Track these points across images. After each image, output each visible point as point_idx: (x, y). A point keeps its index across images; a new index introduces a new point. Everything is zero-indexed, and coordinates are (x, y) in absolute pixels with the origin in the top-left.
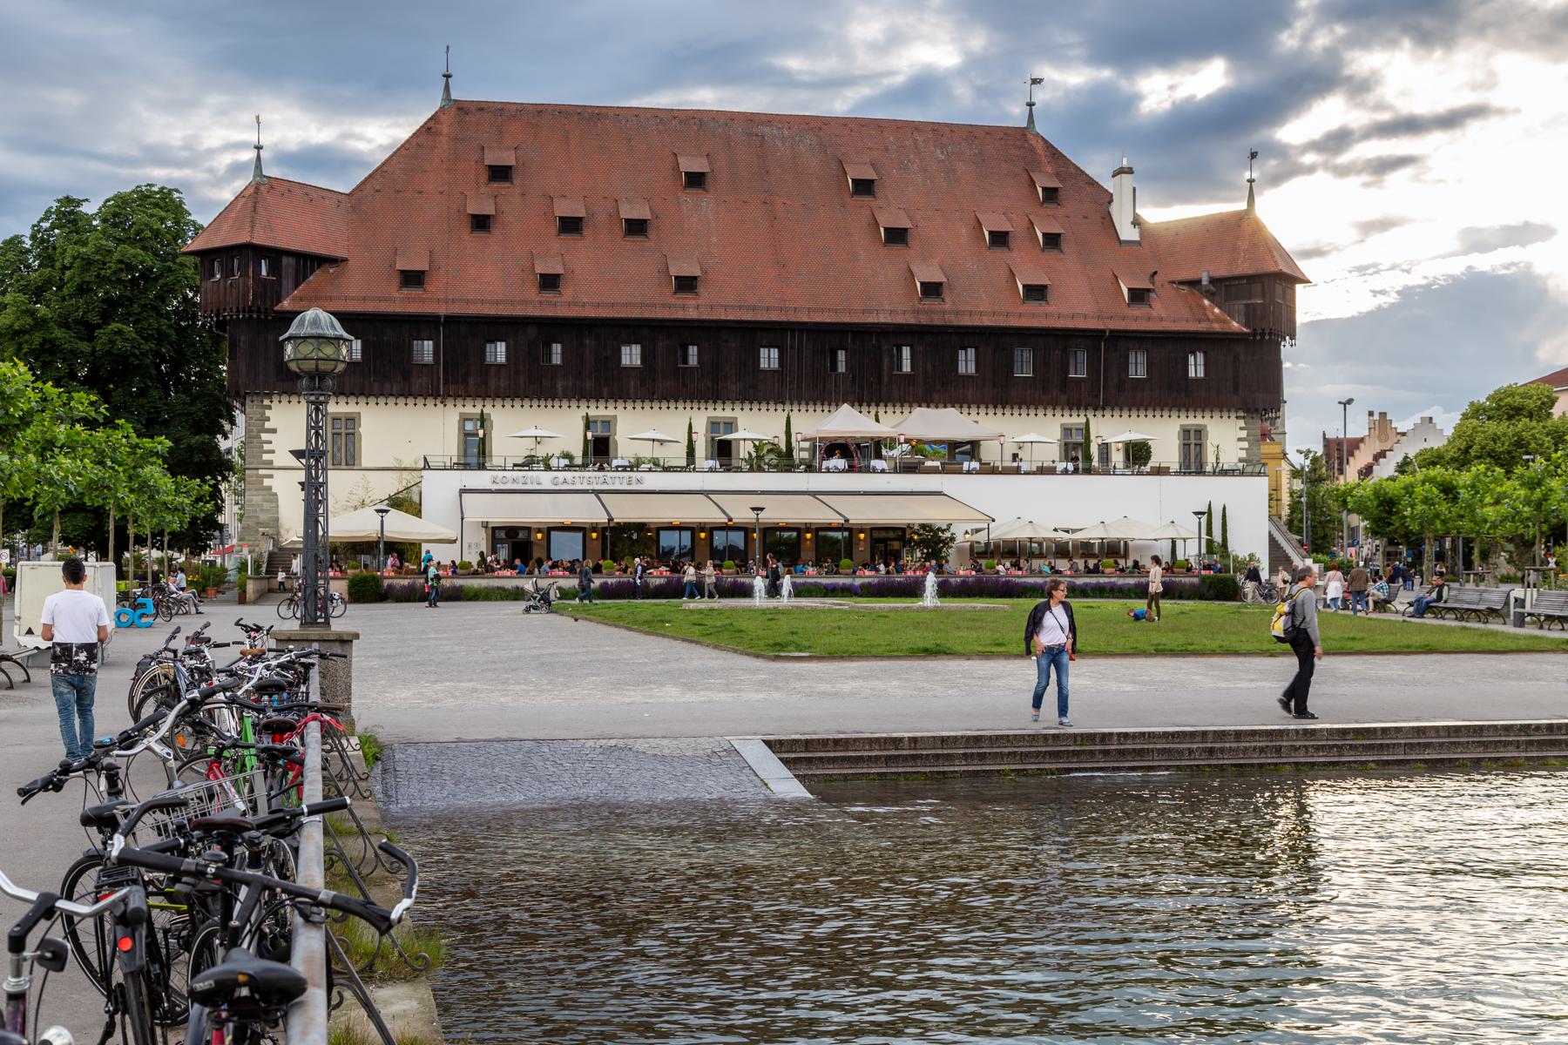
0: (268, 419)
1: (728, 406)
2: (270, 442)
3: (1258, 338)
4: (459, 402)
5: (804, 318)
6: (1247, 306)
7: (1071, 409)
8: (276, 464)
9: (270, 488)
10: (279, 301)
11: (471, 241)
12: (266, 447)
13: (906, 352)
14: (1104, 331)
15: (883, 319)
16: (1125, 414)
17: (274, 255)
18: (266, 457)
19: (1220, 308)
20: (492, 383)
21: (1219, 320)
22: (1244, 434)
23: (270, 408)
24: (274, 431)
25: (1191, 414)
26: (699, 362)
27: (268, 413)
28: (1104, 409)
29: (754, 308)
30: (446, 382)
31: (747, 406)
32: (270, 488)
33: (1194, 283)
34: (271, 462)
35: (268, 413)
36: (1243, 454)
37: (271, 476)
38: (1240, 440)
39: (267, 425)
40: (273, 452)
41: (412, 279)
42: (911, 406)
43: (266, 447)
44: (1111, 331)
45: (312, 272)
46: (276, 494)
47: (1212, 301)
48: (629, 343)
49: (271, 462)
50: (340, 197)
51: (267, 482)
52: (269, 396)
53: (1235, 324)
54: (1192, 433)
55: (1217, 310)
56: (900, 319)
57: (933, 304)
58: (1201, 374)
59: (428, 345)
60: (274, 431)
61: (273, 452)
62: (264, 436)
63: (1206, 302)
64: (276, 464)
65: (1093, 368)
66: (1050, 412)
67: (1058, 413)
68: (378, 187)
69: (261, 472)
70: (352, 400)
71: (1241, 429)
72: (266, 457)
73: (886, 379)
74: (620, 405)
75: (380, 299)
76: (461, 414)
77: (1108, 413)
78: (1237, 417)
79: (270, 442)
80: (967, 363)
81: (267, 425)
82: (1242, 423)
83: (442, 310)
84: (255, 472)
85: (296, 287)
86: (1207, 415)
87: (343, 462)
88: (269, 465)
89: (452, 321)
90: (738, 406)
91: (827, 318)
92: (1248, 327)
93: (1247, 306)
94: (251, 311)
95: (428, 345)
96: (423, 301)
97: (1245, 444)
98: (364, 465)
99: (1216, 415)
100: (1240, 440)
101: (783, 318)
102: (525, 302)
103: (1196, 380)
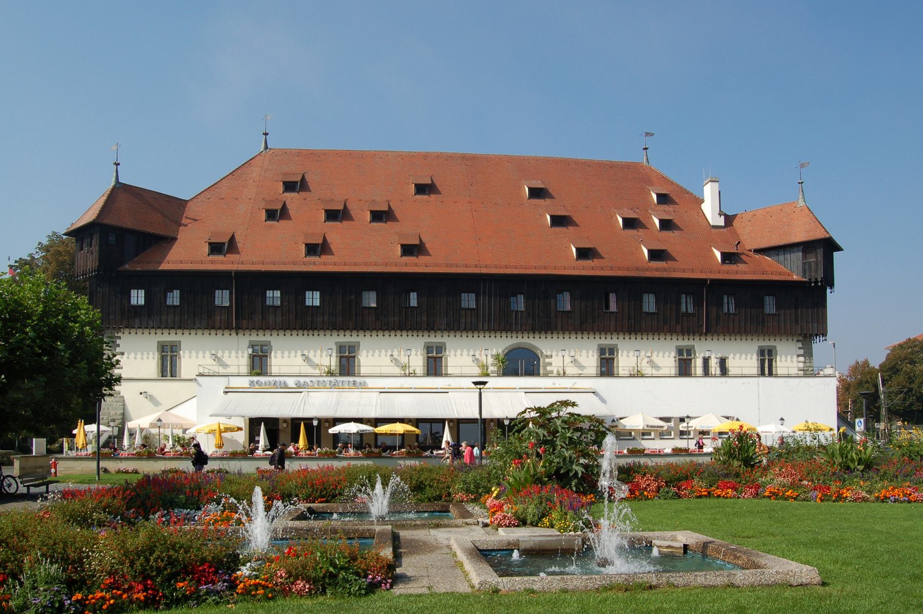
0: (119, 346)
1: (439, 334)
4: (247, 333)
14: (706, 280)
16: (721, 338)
20: (271, 319)
22: (801, 352)
23: (120, 338)
25: (766, 339)
26: (418, 304)
27: (118, 342)
28: (706, 334)
31: (452, 334)
35: (118, 342)
36: (801, 365)
44: (712, 280)
54: (766, 352)
66: (669, 338)
67: (674, 338)
71: (800, 348)
76: (250, 341)
77: (709, 338)
78: (798, 341)
81: (118, 350)
85: (136, 255)
86: (778, 338)
87: (169, 374)
90: (446, 334)
92: (805, 278)
97: (802, 359)
98: (183, 377)
99: (784, 340)
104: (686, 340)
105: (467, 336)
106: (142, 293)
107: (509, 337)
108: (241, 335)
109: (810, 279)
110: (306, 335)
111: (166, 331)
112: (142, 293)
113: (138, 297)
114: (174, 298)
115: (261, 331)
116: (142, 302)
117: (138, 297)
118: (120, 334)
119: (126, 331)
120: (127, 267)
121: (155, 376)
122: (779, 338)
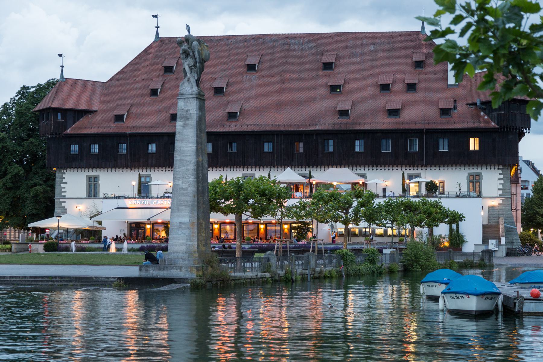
0: (64, 178)
2: (64, 188)
3: (502, 130)
5: (282, 129)
6: (498, 115)
7: (410, 167)
8: (67, 197)
9: (64, 207)
10: (66, 130)
11: (149, 100)
12: (63, 190)
13: (331, 142)
14: (423, 130)
15: (318, 128)
17: (64, 111)
18: (63, 194)
19: (488, 116)
21: (486, 122)
22: (501, 176)
23: (65, 173)
24: (66, 183)
27: (64, 176)
29: (260, 125)
30: (131, 161)
32: (64, 207)
33: (475, 104)
34: (65, 196)
35: (64, 176)
37: (65, 202)
38: (499, 179)
39: (64, 181)
40: (65, 192)
41: (119, 118)
42: (285, 167)
43: (63, 190)
44: (427, 130)
45: (81, 117)
46: (66, 209)
47: (485, 112)
48: (268, 142)
49: (65, 196)
50: (101, 84)
51: (63, 204)
52: (64, 169)
53: (493, 124)
55: (486, 117)
56: (325, 128)
57: (345, 120)
58: (477, 148)
59: (125, 146)
60: (66, 183)
61: (65, 192)
62: (63, 185)
63: (482, 113)
64: (67, 197)
65: (420, 147)
68: (118, 79)
69: (61, 200)
70: (94, 170)
71: (500, 174)
72: (63, 194)
73: (320, 156)
74: (152, 170)
75: (105, 128)
77: (429, 169)
78: (498, 169)
79: (64, 188)
80: (358, 146)
81: (64, 181)
82: (500, 171)
83: (128, 131)
84: (59, 200)
87: (93, 195)
88: (64, 197)
89: (132, 135)
91: (292, 129)
93: (498, 115)
94: (52, 134)
95: (125, 146)
96: (122, 127)
97: (502, 182)
100: (499, 179)
101: (272, 129)
102: (222, 125)
103: (474, 151)
104: (415, 170)
105: (381, 170)
106: (77, 146)
107: (232, 170)
108: (133, 171)
109: (501, 126)
110: (170, 171)
111: (90, 170)
112: (77, 146)
113: (75, 149)
114: (95, 149)
115: (87, 168)
116: (77, 152)
117: (75, 149)
118: (65, 171)
119: (68, 170)
120: (69, 131)
121: (85, 196)
122: (425, 168)
